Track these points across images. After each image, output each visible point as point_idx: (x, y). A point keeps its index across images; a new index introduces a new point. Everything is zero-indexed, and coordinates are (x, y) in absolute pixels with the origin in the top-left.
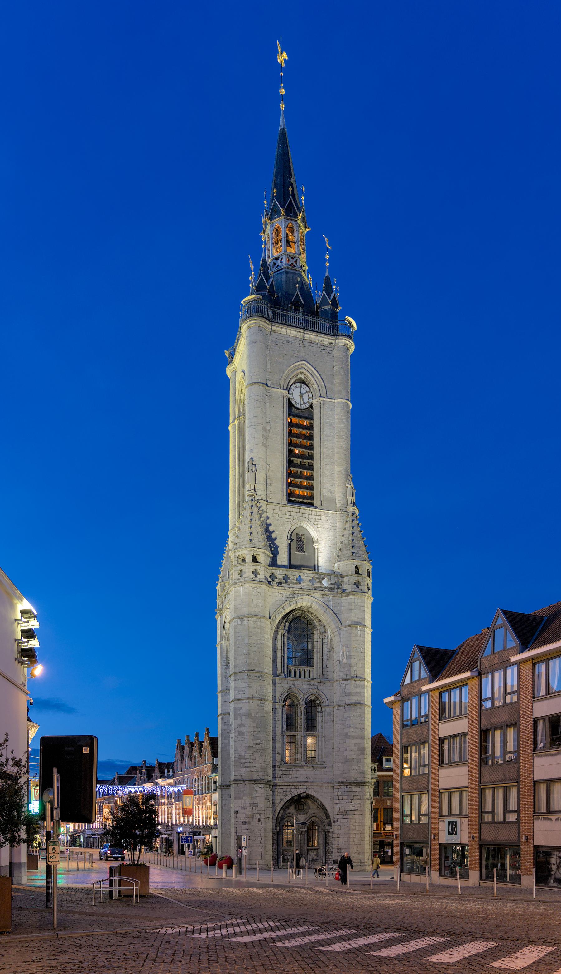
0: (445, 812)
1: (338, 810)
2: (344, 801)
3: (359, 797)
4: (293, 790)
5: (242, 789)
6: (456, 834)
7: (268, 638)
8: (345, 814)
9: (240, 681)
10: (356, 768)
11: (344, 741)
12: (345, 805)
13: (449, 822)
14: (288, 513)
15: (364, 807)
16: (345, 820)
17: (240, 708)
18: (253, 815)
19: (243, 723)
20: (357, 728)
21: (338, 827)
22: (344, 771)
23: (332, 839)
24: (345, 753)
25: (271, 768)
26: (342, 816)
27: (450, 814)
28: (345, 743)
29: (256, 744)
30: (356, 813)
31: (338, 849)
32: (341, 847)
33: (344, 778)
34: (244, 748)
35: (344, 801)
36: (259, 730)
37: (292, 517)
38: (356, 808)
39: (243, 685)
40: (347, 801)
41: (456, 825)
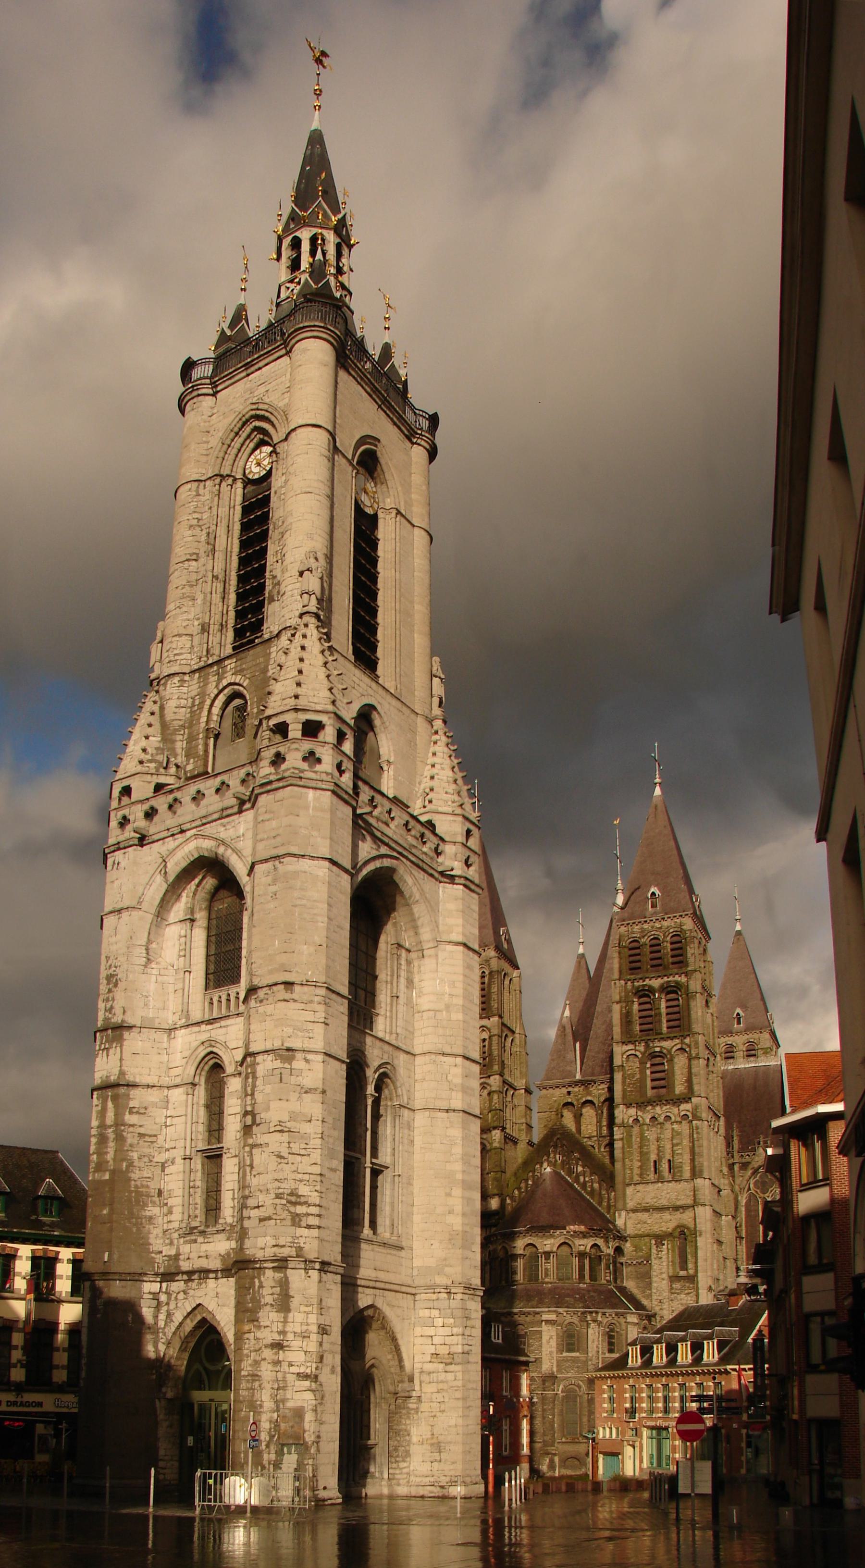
2: (447, 1331)
8: (449, 1361)
11: (448, 1190)
12: (449, 1340)
16: (450, 1377)
22: (445, 1259)
23: (408, 1422)
26: (441, 1366)
28: (449, 1195)
31: (432, 1445)
32: (441, 1438)
35: (447, 1331)
39: (309, 1016)
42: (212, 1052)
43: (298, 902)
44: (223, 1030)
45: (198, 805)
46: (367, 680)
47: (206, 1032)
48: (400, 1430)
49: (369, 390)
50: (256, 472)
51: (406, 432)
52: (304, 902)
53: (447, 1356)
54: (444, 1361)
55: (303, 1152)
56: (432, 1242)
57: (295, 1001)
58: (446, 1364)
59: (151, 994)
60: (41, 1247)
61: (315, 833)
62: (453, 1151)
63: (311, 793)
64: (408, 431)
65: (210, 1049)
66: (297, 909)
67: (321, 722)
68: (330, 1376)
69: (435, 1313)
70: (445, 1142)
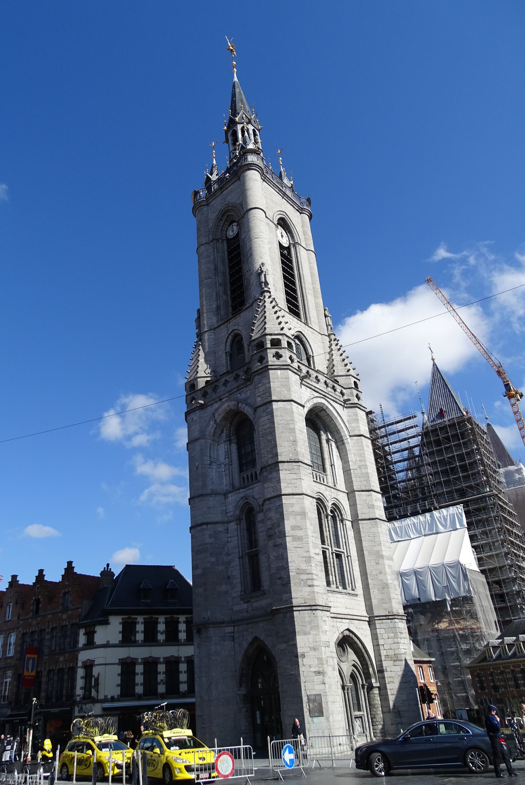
1: (385, 654)
2: (390, 641)
5: (307, 619)
8: (395, 659)
9: (289, 472)
12: (393, 646)
17: (292, 505)
19: (298, 524)
21: (390, 680)
24: (380, 577)
26: (392, 662)
28: (378, 563)
33: (385, 609)
34: (304, 559)
38: (406, 651)
39: (294, 476)
40: (395, 640)
42: (247, 502)
43: (280, 422)
44: (251, 490)
45: (226, 387)
46: (296, 320)
47: (243, 493)
48: (375, 704)
49: (277, 191)
50: (231, 234)
51: (297, 208)
52: (283, 422)
53: (393, 656)
54: (393, 659)
55: (300, 546)
56: (374, 590)
57: (286, 470)
59: (214, 477)
60: (169, 616)
61: (283, 389)
62: (376, 540)
63: (279, 371)
64: (298, 207)
65: (246, 501)
66: (280, 425)
67: (279, 339)
68: (333, 672)
69: (382, 631)
70: (371, 535)
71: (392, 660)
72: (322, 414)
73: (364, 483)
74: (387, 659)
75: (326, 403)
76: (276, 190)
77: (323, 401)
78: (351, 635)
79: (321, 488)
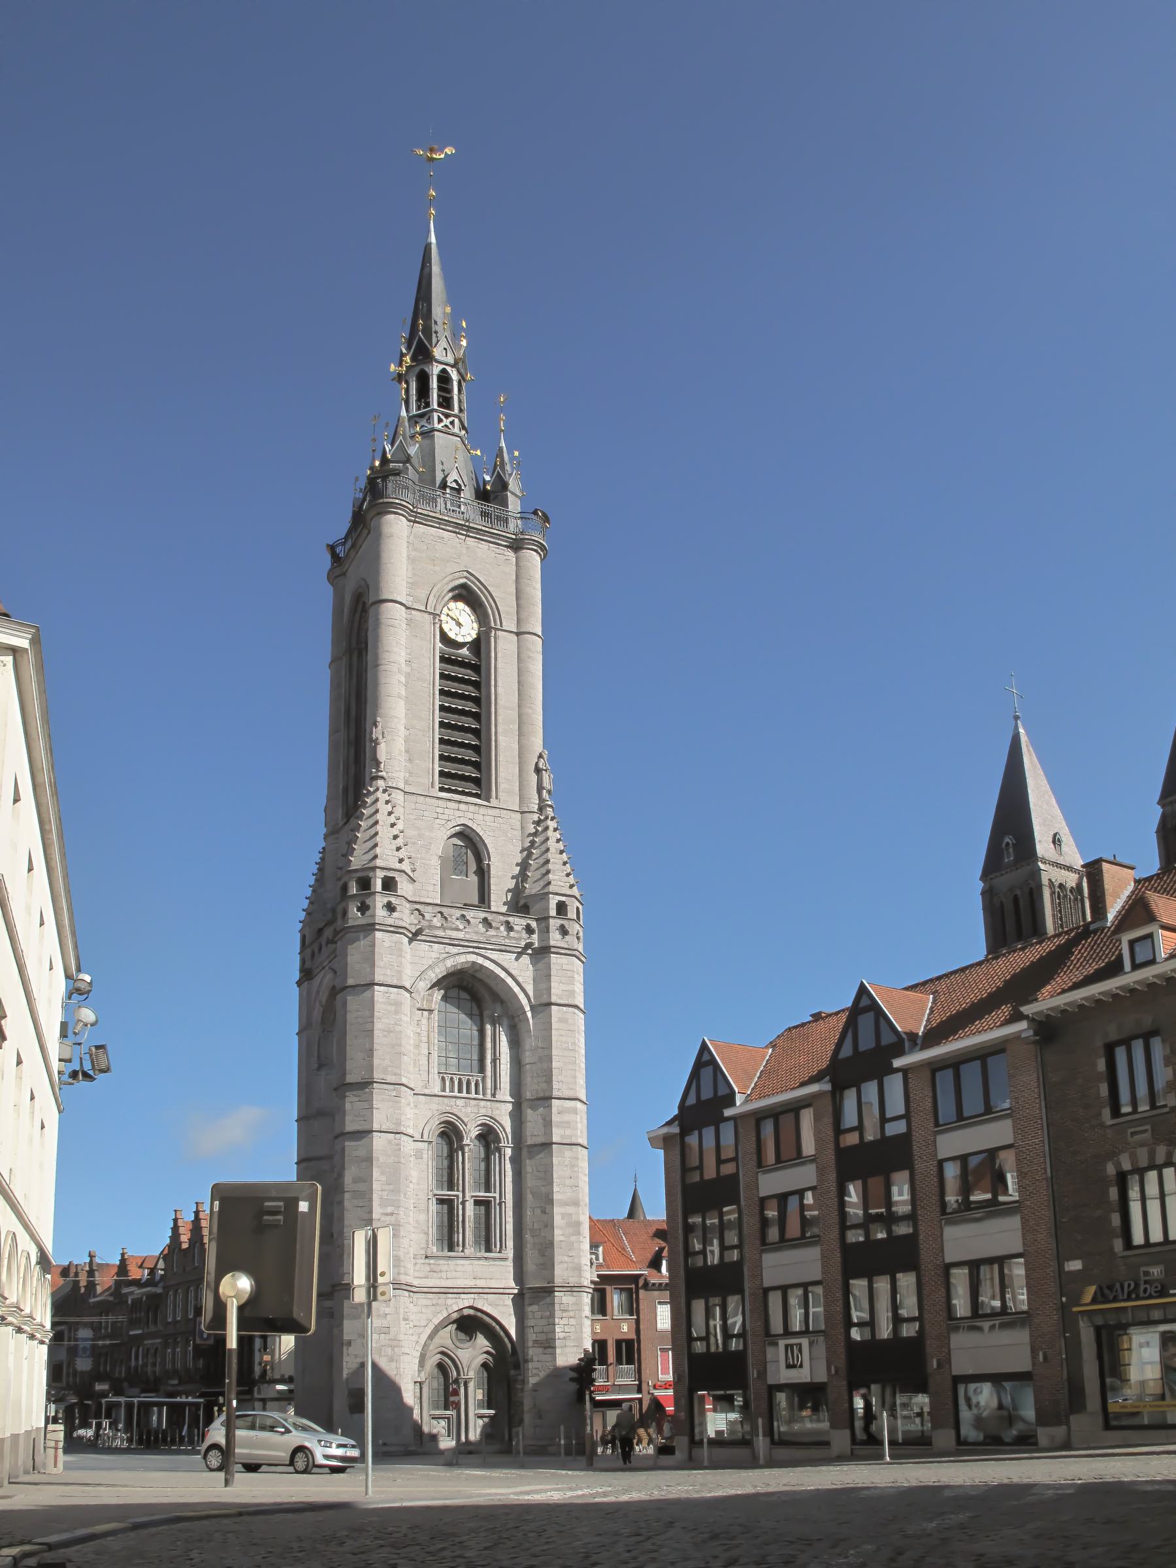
0: (777, 1326)
3: (571, 1314)
4: (449, 1302)
6: (801, 1366)
7: (407, 1022)
8: (546, 1345)
10: (566, 1259)
13: (787, 1346)
14: (439, 810)
15: (582, 1332)
18: (381, 1349)
20: (565, 1185)
25: (412, 1259)
27: (787, 1333)
28: (544, 1212)
29: (387, 1214)
30: (568, 1343)
36: (391, 1187)
37: (446, 817)
38: (568, 1334)
41: (800, 1351)
55: (361, 1205)
58: (545, 1348)
71: (540, 1347)
72: (478, 975)
73: (544, 1086)
74: (536, 1345)
75: (480, 960)
76: (448, 528)
77: (472, 958)
78: (479, 1314)
79: (453, 1104)
